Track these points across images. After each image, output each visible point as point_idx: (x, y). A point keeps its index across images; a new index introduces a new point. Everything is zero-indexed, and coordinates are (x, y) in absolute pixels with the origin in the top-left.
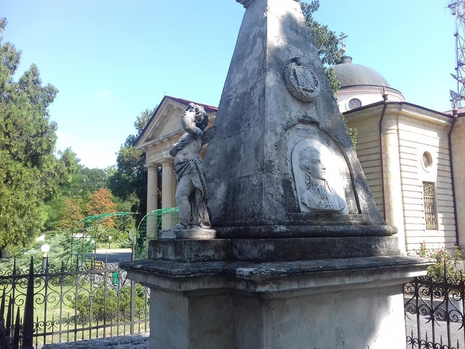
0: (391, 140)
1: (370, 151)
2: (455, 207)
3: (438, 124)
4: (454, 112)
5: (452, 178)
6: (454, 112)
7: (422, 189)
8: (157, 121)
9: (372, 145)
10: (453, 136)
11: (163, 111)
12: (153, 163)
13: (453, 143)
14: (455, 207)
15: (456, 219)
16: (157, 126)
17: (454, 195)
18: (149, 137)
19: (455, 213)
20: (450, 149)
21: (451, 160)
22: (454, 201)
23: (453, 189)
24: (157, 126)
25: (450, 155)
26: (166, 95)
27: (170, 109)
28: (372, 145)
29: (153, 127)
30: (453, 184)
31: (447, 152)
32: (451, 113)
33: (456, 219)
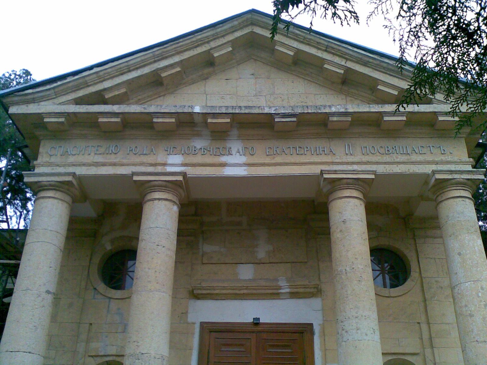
11: (213, 44)
12: (80, 179)
16: (163, 75)
18: (108, 96)
24: (163, 75)
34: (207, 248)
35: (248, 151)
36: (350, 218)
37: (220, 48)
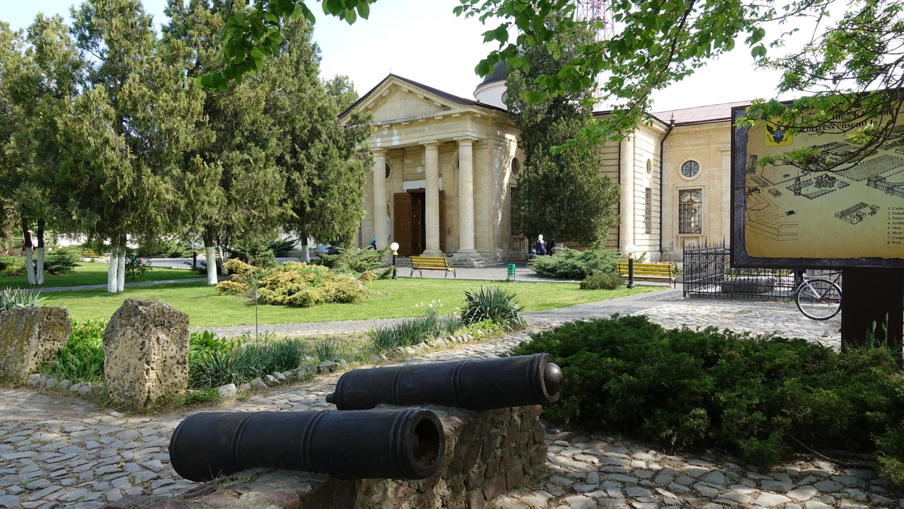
0: (628, 146)
1: (607, 157)
2: (661, 212)
3: (657, 131)
4: (672, 121)
5: (661, 185)
6: (672, 121)
7: (644, 195)
8: (371, 101)
9: (610, 150)
10: (665, 144)
13: (664, 150)
14: (661, 212)
15: (661, 223)
17: (661, 201)
19: (661, 218)
20: (661, 157)
21: (661, 168)
22: (661, 207)
23: (661, 196)
25: (661, 162)
26: (393, 73)
27: (394, 89)
28: (610, 150)
29: (363, 108)
30: (661, 190)
31: (659, 159)
32: (669, 123)
33: (661, 223)
34: (407, 162)
35: (399, 134)
36: (431, 155)
37: (384, 91)
